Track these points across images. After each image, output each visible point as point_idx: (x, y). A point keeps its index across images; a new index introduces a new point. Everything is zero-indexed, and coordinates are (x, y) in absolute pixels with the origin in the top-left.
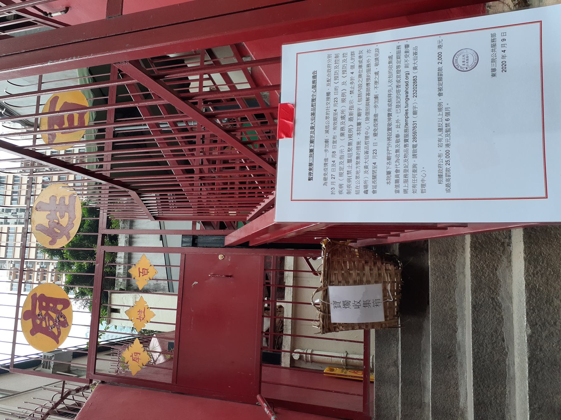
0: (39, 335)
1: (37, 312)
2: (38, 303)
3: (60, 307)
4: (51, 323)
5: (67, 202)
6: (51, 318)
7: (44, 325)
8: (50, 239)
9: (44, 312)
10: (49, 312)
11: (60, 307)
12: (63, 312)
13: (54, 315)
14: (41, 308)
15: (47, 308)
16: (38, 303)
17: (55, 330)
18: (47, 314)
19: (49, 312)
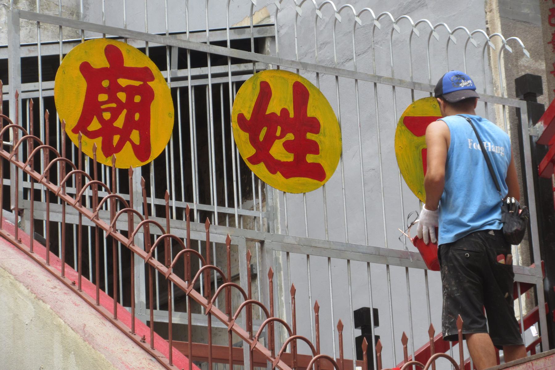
0: (83, 85)
1: (123, 82)
2: (137, 83)
3: (135, 136)
4: (107, 116)
5: (310, 158)
6: (115, 114)
7: (103, 97)
8: (248, 116)
9: (122, 96)
10: (125, 112)
11: (135, 136)
12: (128, 146)
13: (119, 123)
14: (130, 91)
15: (130, 105)
16: (137, 83)
17: (95, 125)
18: (121, 106)
19: (125, 112)
